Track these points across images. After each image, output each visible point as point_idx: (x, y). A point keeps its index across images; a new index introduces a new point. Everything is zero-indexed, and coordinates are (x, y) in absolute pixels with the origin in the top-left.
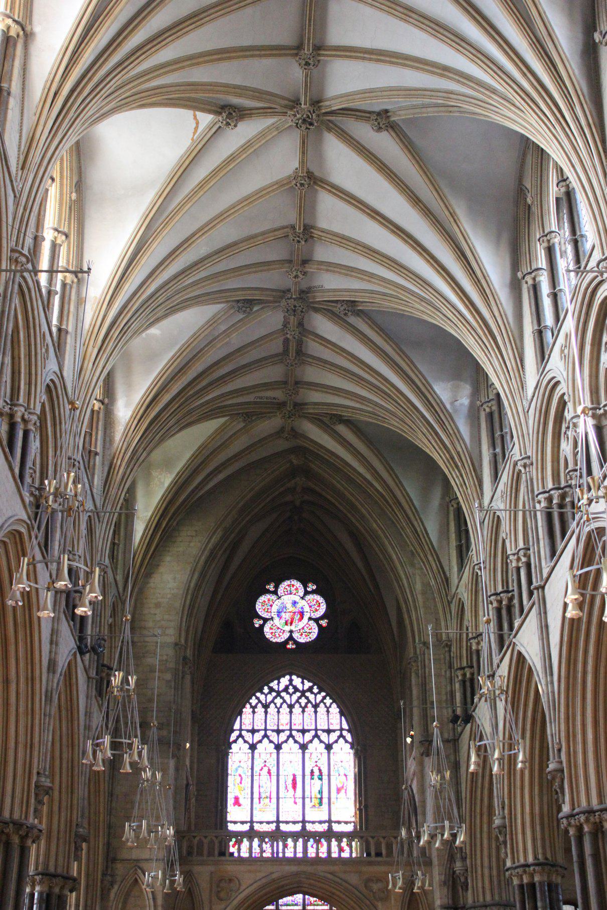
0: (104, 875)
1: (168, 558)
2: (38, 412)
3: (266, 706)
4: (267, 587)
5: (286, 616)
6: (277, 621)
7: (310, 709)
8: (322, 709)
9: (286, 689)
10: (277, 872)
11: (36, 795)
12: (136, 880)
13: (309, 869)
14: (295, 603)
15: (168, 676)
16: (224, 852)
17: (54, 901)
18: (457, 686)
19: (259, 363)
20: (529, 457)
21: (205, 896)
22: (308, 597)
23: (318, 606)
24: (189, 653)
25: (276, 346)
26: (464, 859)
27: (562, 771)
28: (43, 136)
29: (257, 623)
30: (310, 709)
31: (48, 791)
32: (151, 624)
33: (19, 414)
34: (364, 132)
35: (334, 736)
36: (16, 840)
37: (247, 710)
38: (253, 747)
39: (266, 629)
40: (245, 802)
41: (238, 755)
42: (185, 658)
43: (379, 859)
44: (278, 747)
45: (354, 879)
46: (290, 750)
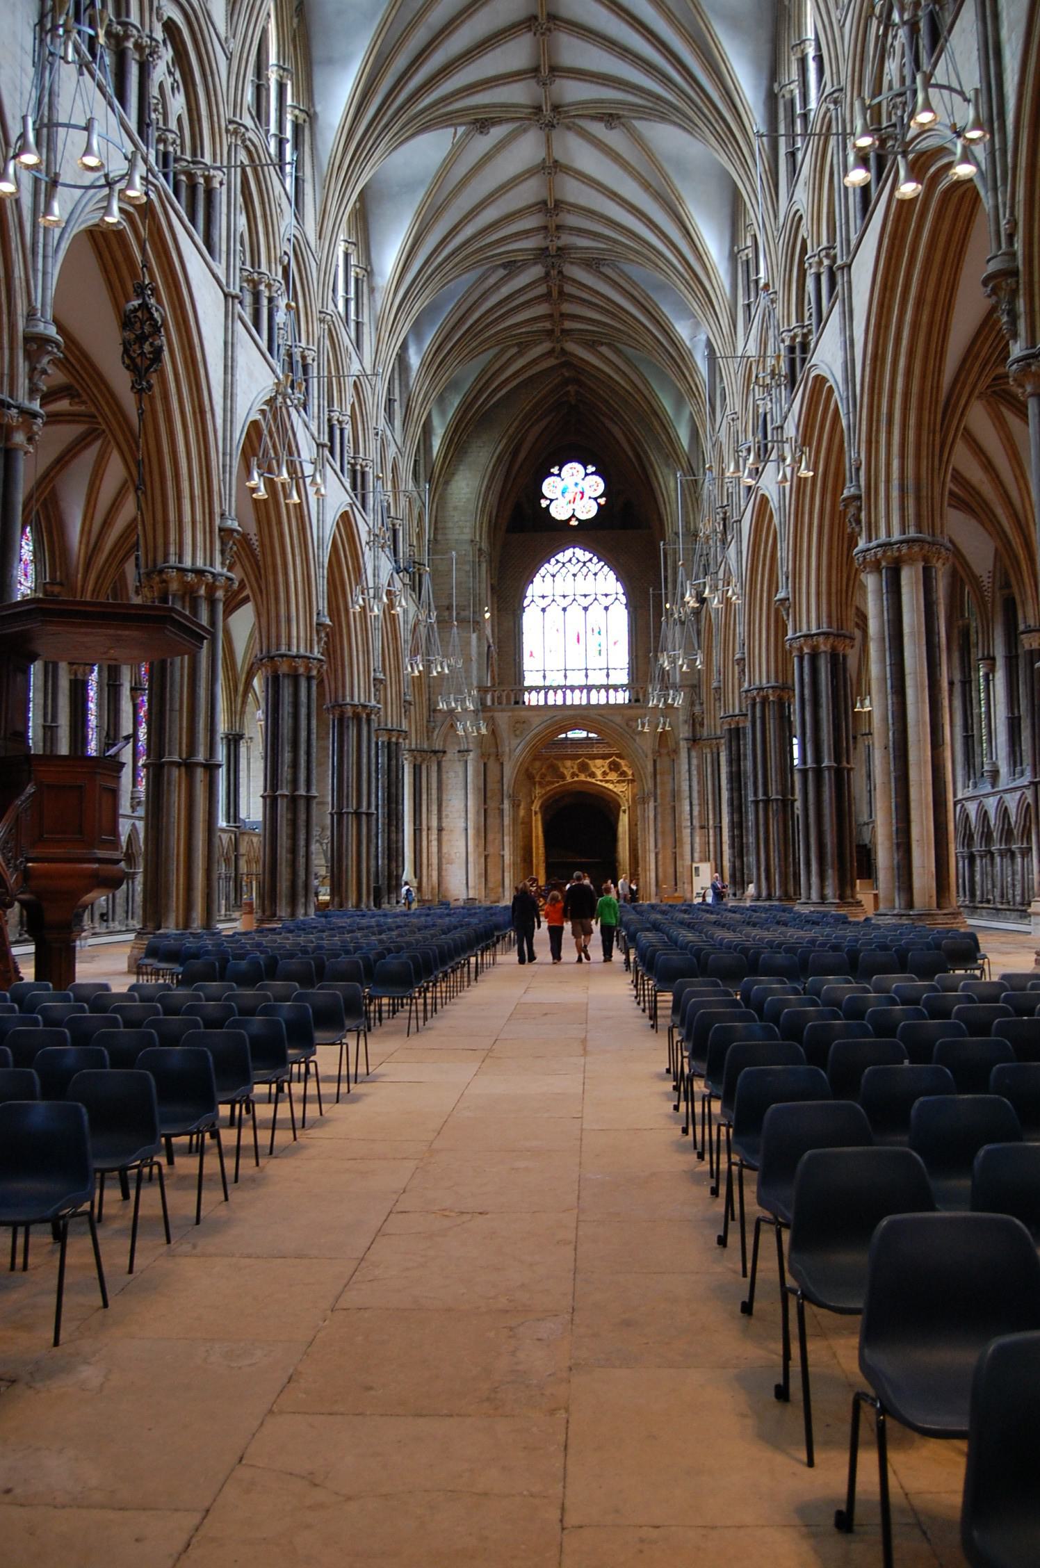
0: (428, 721)
1: (461, 468)
2: (349, 413)
4: (552, 470)
5: (570, 496)
9: (570, 561)
11: (375, 685)
12: (452, 726)
13: (585, 713)
14: (576, 484)
15: (467, 568)
16: (519, 702)
17: (394, 747)
18: (701, 568)
19: (527, 304)
20: (736, 413)
21: (505, 735)
22: (588, 478)
24: (484, 546)
25: (542, 289)
26: (702, 704)
27: (744, 659)
29: (544, 503)
31: (381, 681)
32: (450, 525)
33: (336, 418)
34: (597, 129)
35: (611, 599)
36: (364, 716)
37: (538, 579)
41: (531, 620)
42: (480, 550)
43: (637, 704)
45: (618, 719)
46: (575, 611)
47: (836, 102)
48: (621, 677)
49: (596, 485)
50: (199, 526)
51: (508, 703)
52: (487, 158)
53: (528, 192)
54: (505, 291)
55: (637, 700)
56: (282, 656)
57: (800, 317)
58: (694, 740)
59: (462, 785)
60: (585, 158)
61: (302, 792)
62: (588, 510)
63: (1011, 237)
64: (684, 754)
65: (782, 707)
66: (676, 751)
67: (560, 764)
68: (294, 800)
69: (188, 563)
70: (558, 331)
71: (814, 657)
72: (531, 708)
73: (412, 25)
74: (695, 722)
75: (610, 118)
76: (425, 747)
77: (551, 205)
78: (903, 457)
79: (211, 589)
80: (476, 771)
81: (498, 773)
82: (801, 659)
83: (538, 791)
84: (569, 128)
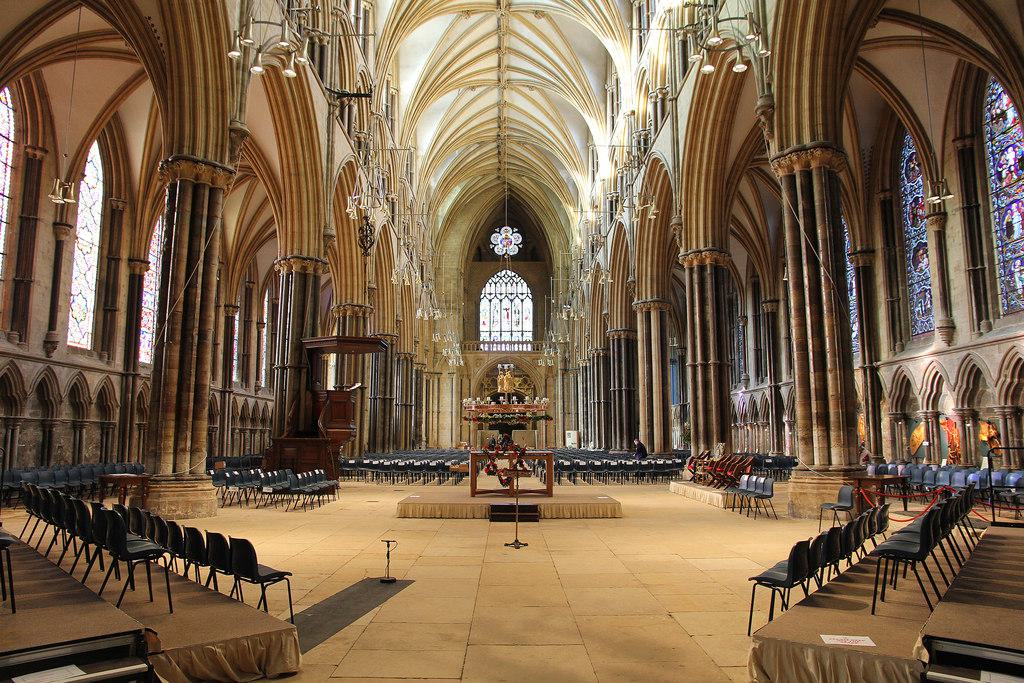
3: (496, 283)
6: (500, 246)
7: (514, 284)
8: (519, 284)
10: (500, 356)
23: (517, 238)
30: (514, 284)
34: (526, 90)
35: (525, 296)
37: (488, 285)
38: (490, 301)
39: (496, 249)
40: (488, 324)
41: (484, 305)
44: (501, 301)
45: (528, 359)
48: (529, 336)
50: (360, 287)
52: (473, 100)
53: (493, 113)
54: (478, 154)
55: (537, 348)
57: (615, 189)
58: (565, 371)
60: (519, 101)
61: (388, 396)
62: (513, 250)
64: (560, 377)
65: (606, 358)
66: (557, 376)
68: (384, 400)
69: (355, 302)
71: (619, 340)
73: (445, 55)
74: (565, 361)
75: (531, 88)
79: (364, 313)
80: (457, 385)
82: (613, 340)
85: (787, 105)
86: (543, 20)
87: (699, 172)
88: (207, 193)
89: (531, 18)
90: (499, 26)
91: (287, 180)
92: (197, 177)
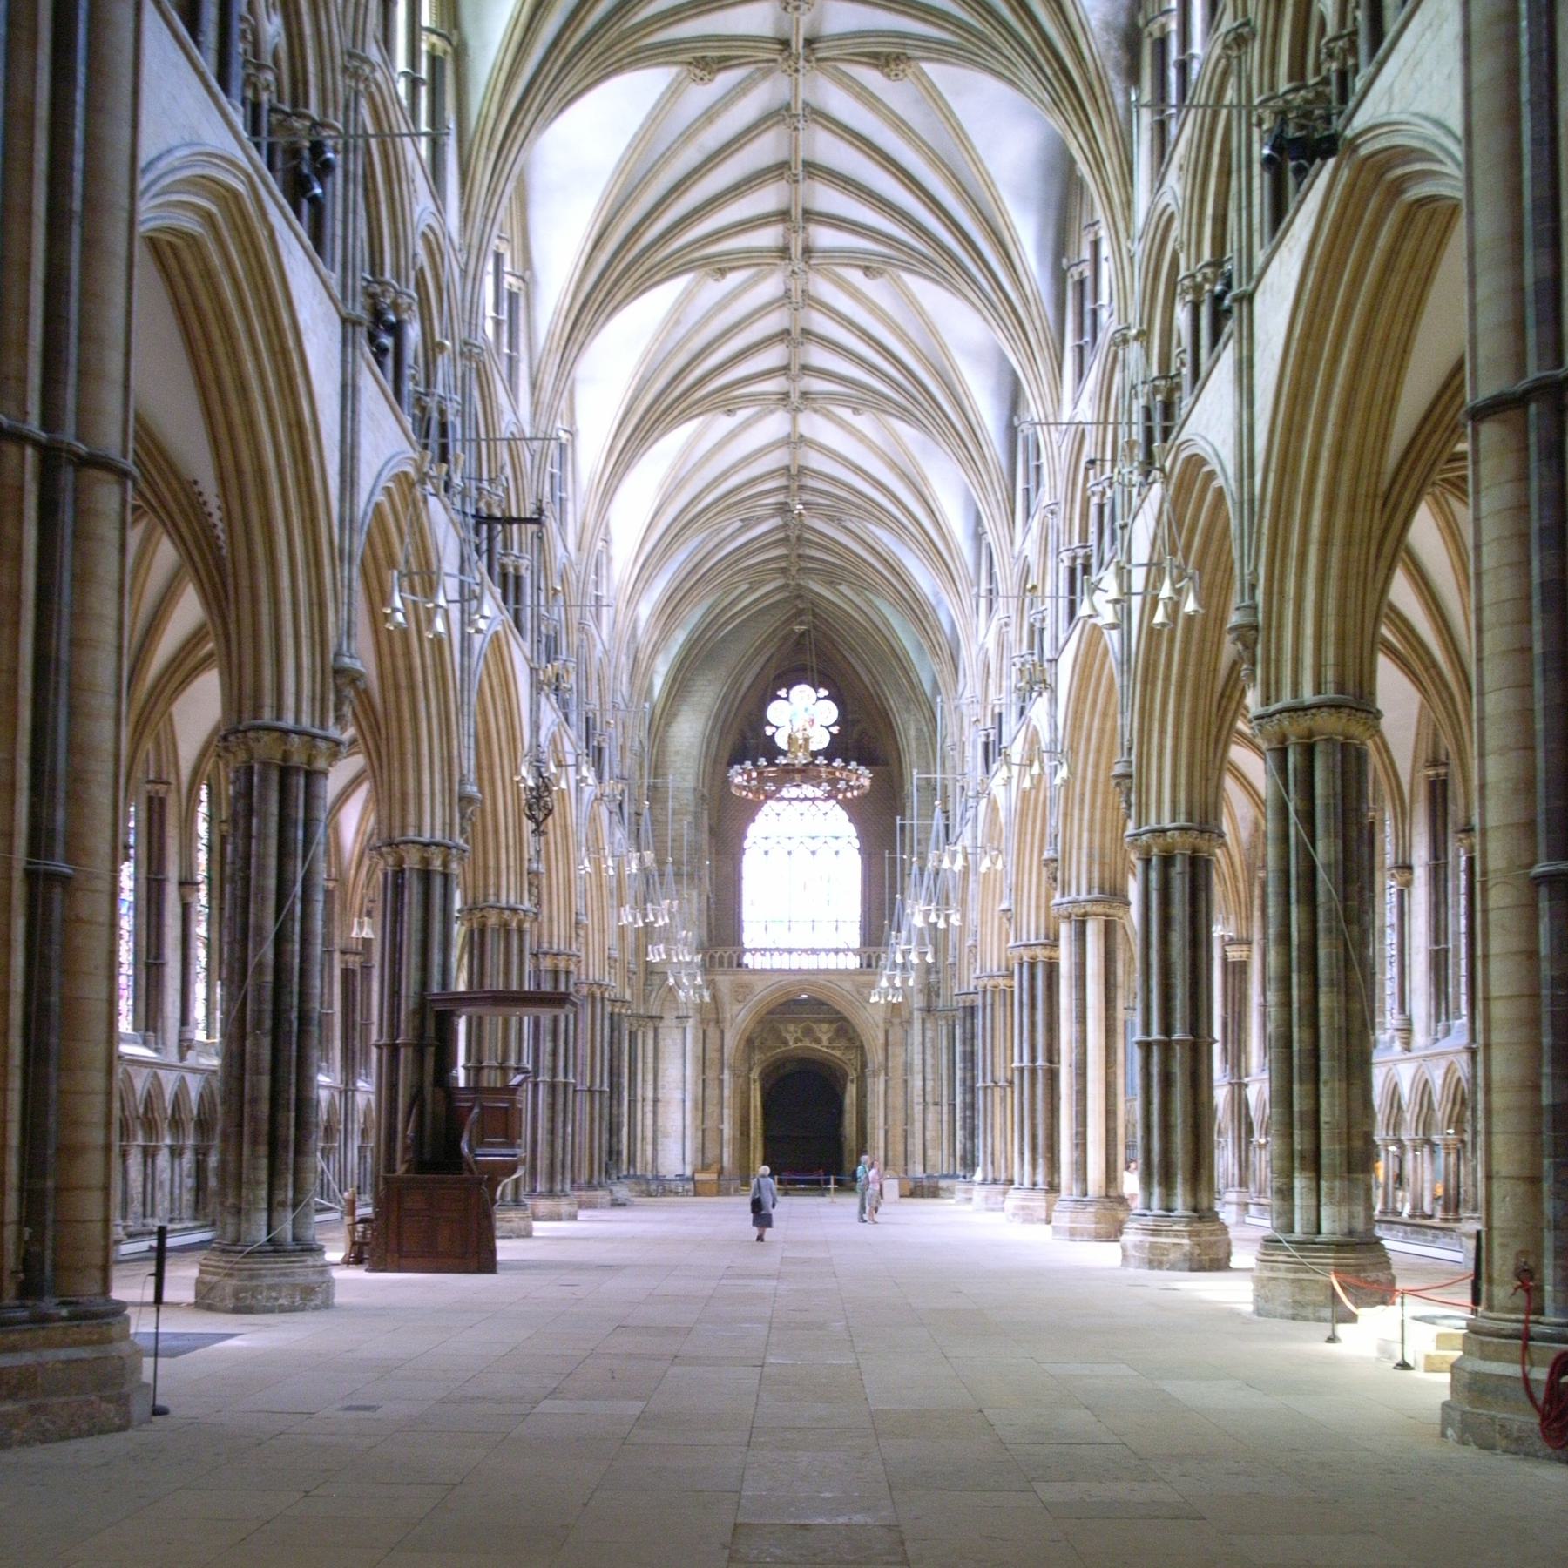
1: (685, 708)
25: (782, 535)
28: (590, 521)
47: (1052, 513)
49: (830, 712)
51: (730, 965)
52: (732, 435)
55: (870, 964)
56: (545, 954)
59: (679, 1054)
63: (1130, 749)
67: (782, 1027)
70: (793, 572)
72: (755, 971)
76: (642, 1012)
77: (794, 471)
78: (1091, 830)
81: (718, 1042)
83: (757, 1056)
84: (815, 411)
85: (1280, 627)
86: (880, 281)
87: (1167, 679)
88: (302, 781)
89: (855, 276)
90: (787, 291)
91: (391, 696)
92: (286, 756)
